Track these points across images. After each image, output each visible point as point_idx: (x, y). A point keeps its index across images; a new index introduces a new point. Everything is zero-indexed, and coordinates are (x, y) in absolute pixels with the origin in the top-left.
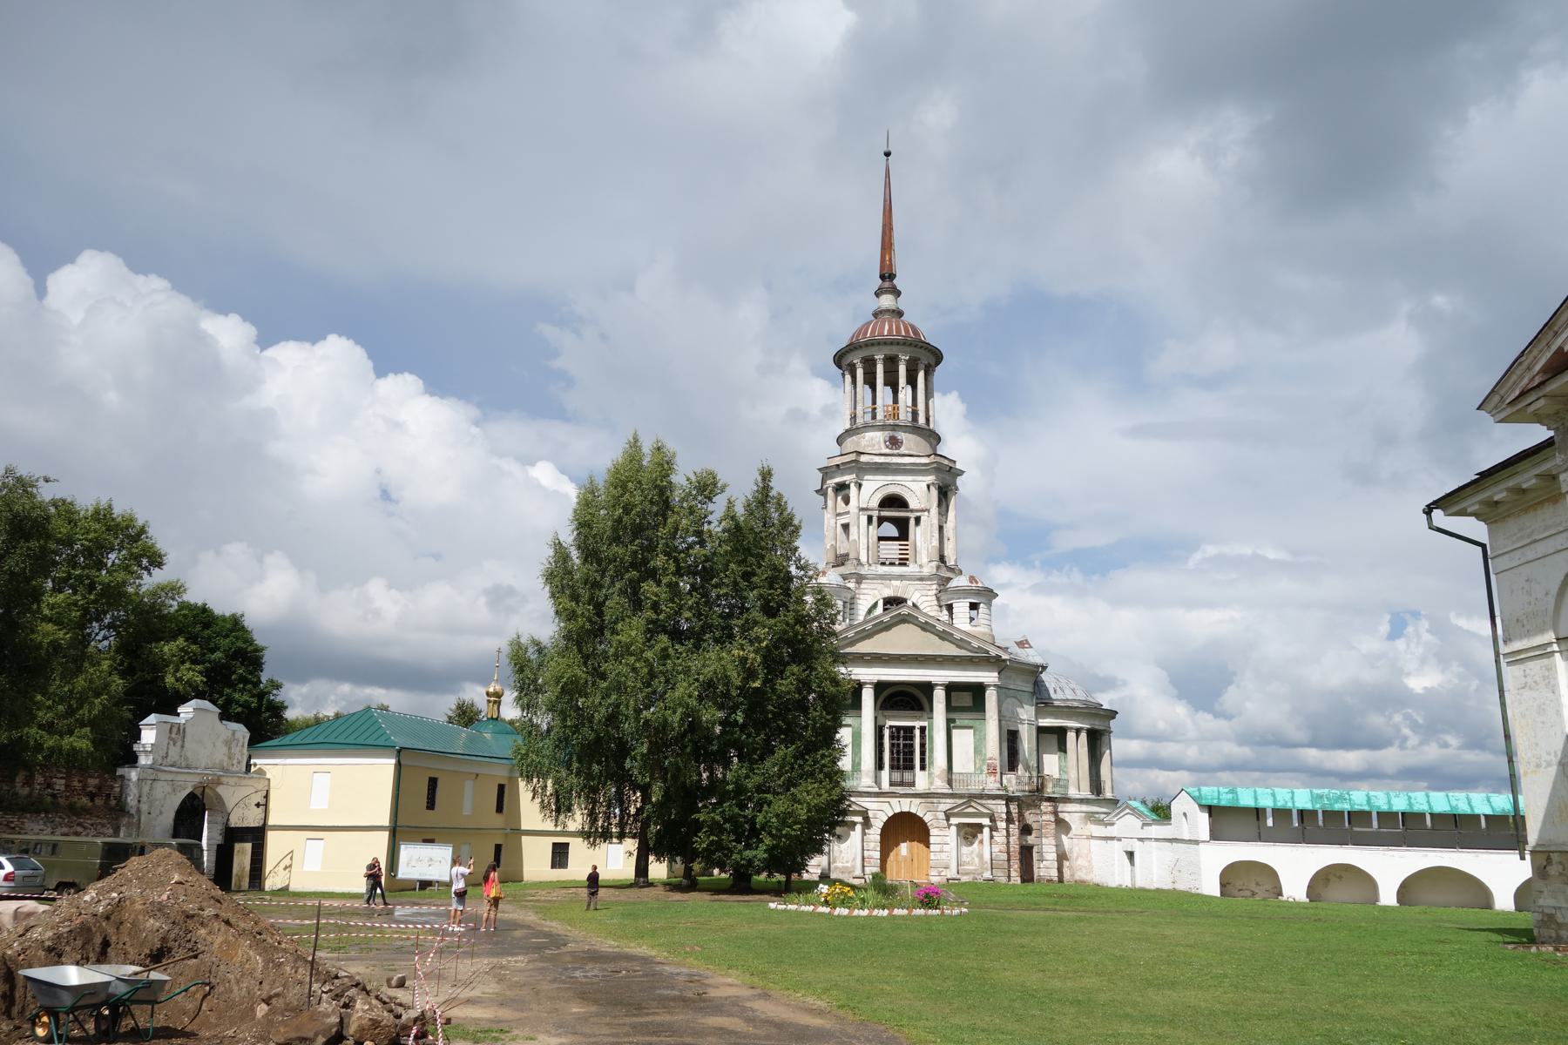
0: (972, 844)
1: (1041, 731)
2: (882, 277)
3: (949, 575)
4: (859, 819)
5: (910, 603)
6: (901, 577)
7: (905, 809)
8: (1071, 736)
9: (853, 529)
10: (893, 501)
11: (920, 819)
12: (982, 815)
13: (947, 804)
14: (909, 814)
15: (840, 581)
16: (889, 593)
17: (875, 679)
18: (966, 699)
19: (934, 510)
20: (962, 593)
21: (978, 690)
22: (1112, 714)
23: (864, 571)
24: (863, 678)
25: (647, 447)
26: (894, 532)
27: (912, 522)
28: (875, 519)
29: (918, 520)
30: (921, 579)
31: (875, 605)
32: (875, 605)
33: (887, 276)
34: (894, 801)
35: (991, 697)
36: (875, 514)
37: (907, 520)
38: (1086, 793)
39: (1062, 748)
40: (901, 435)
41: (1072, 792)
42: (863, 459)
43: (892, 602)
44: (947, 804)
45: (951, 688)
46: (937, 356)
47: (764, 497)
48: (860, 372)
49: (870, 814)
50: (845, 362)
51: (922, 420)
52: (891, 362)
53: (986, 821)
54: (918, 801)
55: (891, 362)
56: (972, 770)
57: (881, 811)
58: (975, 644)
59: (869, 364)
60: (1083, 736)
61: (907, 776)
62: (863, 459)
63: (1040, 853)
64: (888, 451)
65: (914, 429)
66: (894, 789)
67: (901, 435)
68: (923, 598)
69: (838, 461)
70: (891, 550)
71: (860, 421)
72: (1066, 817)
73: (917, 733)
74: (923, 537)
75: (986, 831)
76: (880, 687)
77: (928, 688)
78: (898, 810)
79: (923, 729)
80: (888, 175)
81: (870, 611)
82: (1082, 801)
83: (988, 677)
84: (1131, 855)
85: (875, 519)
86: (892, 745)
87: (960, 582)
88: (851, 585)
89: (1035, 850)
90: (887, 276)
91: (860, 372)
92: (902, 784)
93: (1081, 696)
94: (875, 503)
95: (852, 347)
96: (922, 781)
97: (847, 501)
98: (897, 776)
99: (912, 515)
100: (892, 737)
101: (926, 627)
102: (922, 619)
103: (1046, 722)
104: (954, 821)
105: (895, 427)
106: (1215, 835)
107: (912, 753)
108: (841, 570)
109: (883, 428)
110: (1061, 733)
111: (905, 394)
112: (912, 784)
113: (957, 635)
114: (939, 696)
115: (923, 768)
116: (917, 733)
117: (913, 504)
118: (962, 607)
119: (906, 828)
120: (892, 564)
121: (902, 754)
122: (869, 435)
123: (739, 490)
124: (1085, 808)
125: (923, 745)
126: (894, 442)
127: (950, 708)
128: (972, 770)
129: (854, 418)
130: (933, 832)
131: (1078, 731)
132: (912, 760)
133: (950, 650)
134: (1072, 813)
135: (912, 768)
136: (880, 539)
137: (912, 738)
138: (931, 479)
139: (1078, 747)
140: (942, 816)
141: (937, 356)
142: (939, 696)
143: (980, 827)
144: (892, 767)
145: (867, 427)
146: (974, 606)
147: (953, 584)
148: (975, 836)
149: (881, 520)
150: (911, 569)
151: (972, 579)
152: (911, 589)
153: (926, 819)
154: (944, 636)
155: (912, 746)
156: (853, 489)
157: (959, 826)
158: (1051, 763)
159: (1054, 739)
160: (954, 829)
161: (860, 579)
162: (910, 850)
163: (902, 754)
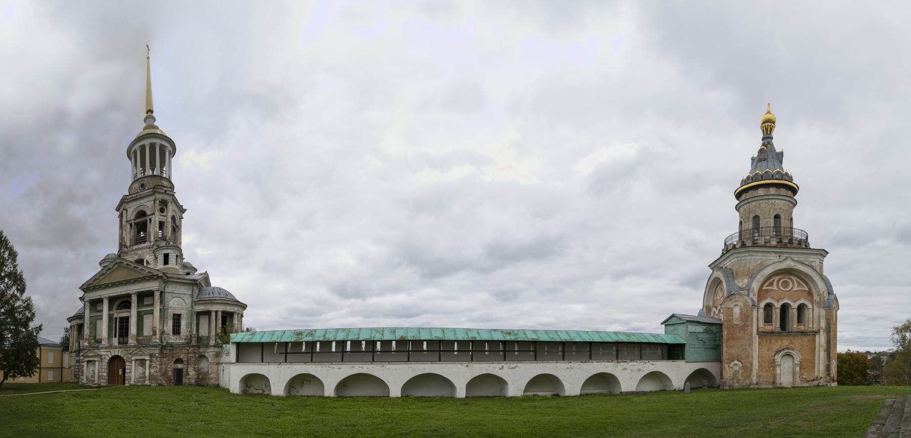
1: (199, 314)
4: (96, 359)
8: (213, 314)
16: (136, 257)
19: (157, 213)
21: (150, 294)
29: (150, 220)
53: (147, 358)
60: (220, 314)
74: (153, 228)
75: (148, 363)
86: (120, 326)
98: (121, 339)
100: (120, 322)
103: (200, 308)
110: (208, 313)
117: (148, 213)
130: (127, 364)
138: (152, 198)
143: (145, 360)
144: (120, 336)
163: (121, 328)
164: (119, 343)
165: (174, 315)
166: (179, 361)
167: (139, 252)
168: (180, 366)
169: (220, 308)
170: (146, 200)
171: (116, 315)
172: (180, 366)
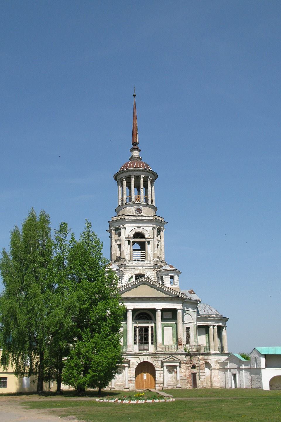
0: (172, 373)
1: (199, 327)
2: (133, 144)
3: (161, 264)
4: (126, 365)
5: (146, 276)
6: (142, 266)
7: (145, 360)
8: (211, 328)
9: (123, 247)
10: (139, 235)
11: (151, 364)
12: (176, 362)
13: (161, 358)
14: (147, 362)
15: (117, 268)
16: (137, 272)
17: (133, 307)
18: (169, 315)
20: (167, 272)
22: (227, 319)
23: (125, 263)
24: (128, 307)
25: (38, 214)
26: (139, 247)
27: (147, 243)
28: (131, 242)
29: (149, 242)
30: (150, 266)
31: (132, 277)
32: (132, 277)
33: (135, 144)
34: (141, 357)
35: (180, 313)
36: (131, 240)
37: (144, 242)
38: (218, 351)
39: (207, 332)
40: (142, 208)
41: (212, 351)
42: (126, 217)
43: (139, 276)
44: (161, 358)
45: (163, 311)
46: (156, 176)
47: (87, 236)
48: (125, 182)
49: (131, 363)
50: (118, 178)
51: (150, 202)
52: (137, 178)
53: (178, 364)
54: (150, 357)
55: (137, 178)
56: (172, 343)
57: (135, 362)
58: (173, 292)
59: (129, 179)
60: (216, 328)
61: (146, 347)
62: (126, 217)
63: (199, 376)
64: (136, 214)
65: (148, 205)
66: (140, 352)
67: (142, 208)
68: (151, 274)
69: (116, 218)
70: (138, 254)
71: (125, 202)
72: (209, 361)
73: (150, 329)
75: (178, 368)
76: (134, 311)
77: (154, 311)
78: (142, 361)
79: (152, 328)
80: (135, 118)
81: (129, 280)
82: (215, 354)
83: (178, 306)
84: (235, 375)
85: (131, 242)
86: (140, 334)
87: (167, 267)
88: (122, 269)
89: (197, 374)
90: (135, 144)
91: (125, 182)
92: (144, 350)
93: (214, 312)
94: (131, 235)
95: (121, 172)
96: (152, 348)
97: (120, 235)
98: (142, 347)
99: (147, 240)
100: (139, 331)
101: (152, 286)
102: (151, 283)
104: (165, 364)
105: (139, 205)
106: (267, 366)
107: (148, 337)
108: (118, 263)
109: (134, 205)
110: (207, 327)
111: (142, 192)
112: (148, 350)
113: (166, 289)
114: (159, 313)
115: (152, 343)
116: (150, 329)
117: (147, 236)
118: (167, 278)
119: (146, 368)
120: (138, 260)
121: (144, 338)
122: (128, 208)
123: (77, 232)
124: (216, 357)
125: (152, 334)
126: (139, 211)
127: (163, 319)
128: (172, 343)
129: (122, 201)
130: (157, 369)
131: (214, 326)
132: (148, 340)
133: (162, 295)
134: (212, 360)
135: (148, 343)
136: (134, 250)
137: (148, 331)
139: (213, 332)
140: (160, 362)
141: (156, 176)
142: (159, 313)
143: (175, 367)
144: (141, 343)
145: (128, 205)
146: (172, 277)
147: (163, 268)
148: (173, 371)
149: (134, 242)
150: (146, 262)
151: (171, 266)
152: (147, 270)
153: (154, 364)
154: (159, 289)
155: (147, 334)
156: (123, 231)
157: (167, 366)
158: (202, 340)
159: (204, 330)
160: (165, 368)
161: (126, 266)
162: (147, 377)
164: (139, 351)
165: (186, 328)
166: (194, 367)
167: (140, 268)
168: (195, 371)
169: (217, 324)
170: (145, 225)
171: (135, 325)
172: (195, 371)
